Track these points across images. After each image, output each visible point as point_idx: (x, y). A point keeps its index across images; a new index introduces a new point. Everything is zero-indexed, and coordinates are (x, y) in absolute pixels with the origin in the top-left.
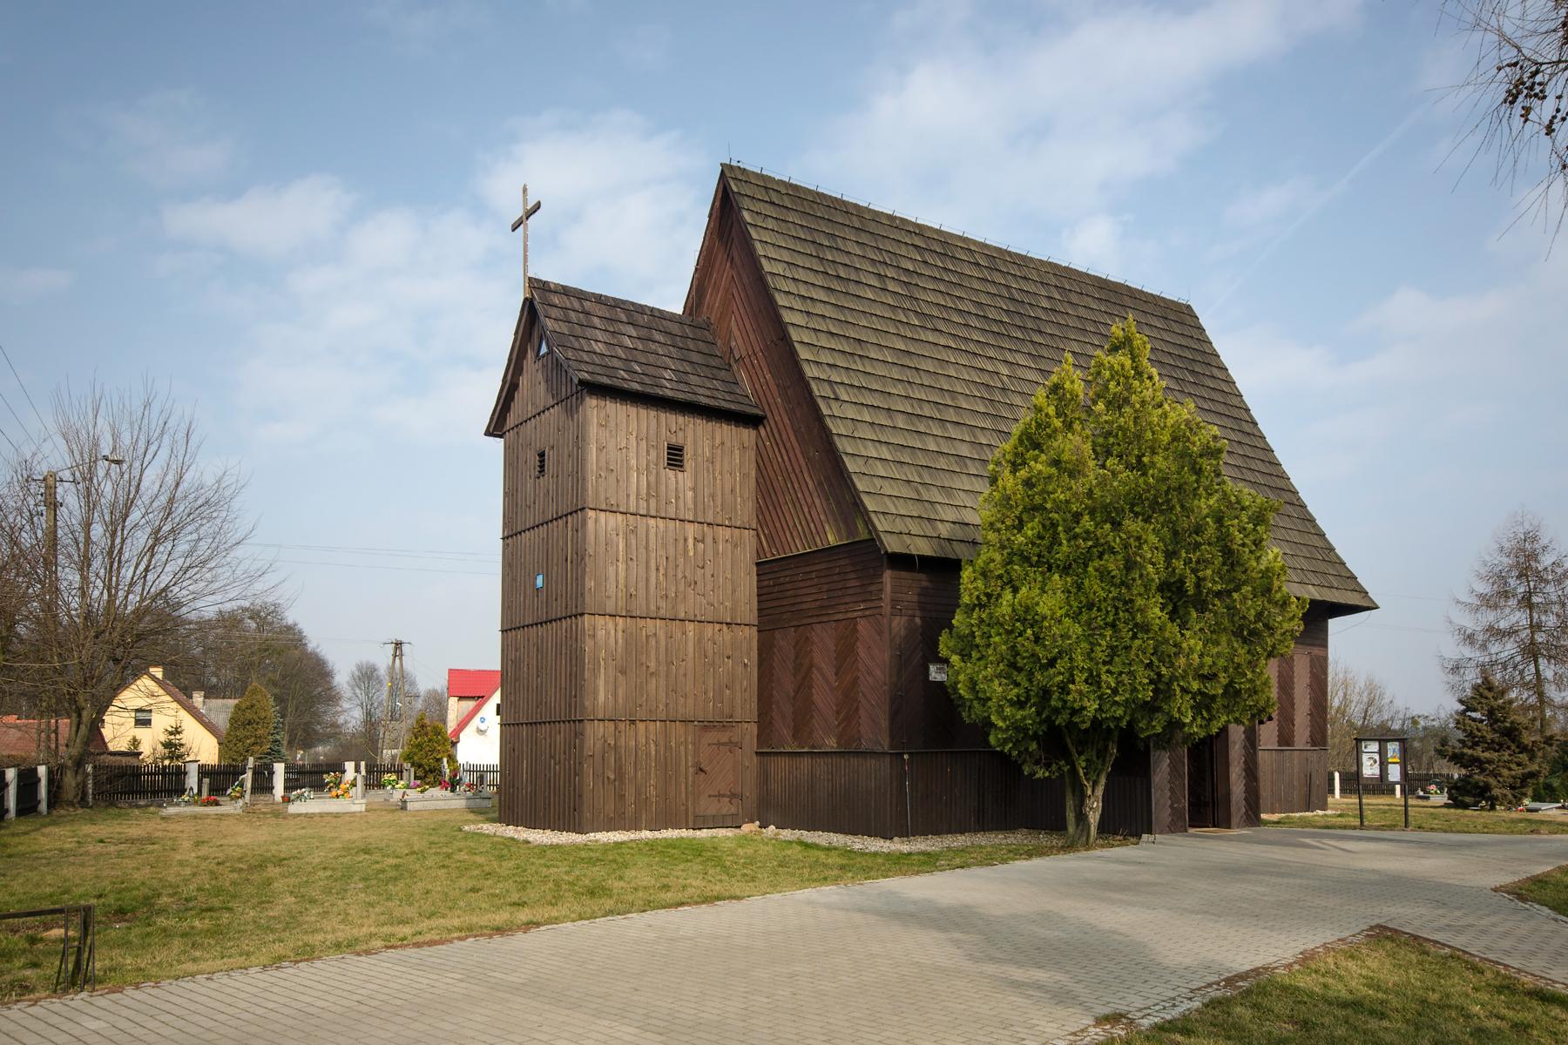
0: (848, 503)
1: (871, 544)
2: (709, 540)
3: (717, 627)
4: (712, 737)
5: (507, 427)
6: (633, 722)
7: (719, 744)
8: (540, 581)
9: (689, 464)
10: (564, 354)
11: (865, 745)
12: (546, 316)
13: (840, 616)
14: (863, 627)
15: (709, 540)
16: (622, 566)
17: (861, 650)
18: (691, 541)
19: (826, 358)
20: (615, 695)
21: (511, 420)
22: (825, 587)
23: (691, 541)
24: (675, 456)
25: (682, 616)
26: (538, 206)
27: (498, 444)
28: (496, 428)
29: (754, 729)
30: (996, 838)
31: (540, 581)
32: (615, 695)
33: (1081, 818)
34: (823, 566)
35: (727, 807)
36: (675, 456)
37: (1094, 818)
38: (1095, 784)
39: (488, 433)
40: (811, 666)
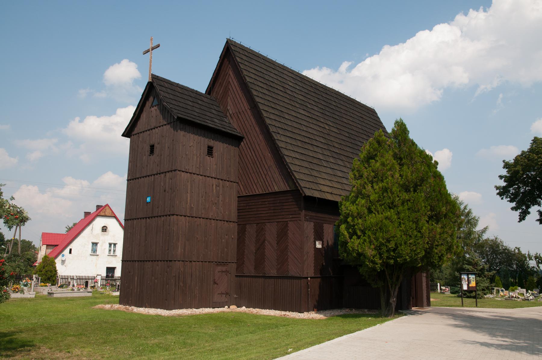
0: (287, 173)
1: (296, 193)
2: (221, 186)
3: (223, 222)
4: (219, 268)
5: (133, 133)
6: (191, 261)
7: (223, 272)
8: (149, 199)
9: (215, 154)
10: (161, 105)
11: (291, 273)
12: (156, 91)
13: (280, 220)
14: (291, 224)
15: (221, 186)
16: (189, 195)
17: (290, 234)
18: (214, 186)
19: (272, 116)
20: (185, 250)
21: (136, 130)
22: (272, 208)
23: (214, 186)
24: (210, 151)
25: (210, 217)
26: (158, 46)
27: (128, 140)
28: (127, 133)
29: (234, 266)
30: (354, 311)
31: (149, 199)
32: (185, 250)
33: (388, 304)
34: (272, 199)
35: (224, 298)
36: (210, 151)
37: (394, 305)
38: (395, 290)
39: (123, 135)
40: (265, 240)
